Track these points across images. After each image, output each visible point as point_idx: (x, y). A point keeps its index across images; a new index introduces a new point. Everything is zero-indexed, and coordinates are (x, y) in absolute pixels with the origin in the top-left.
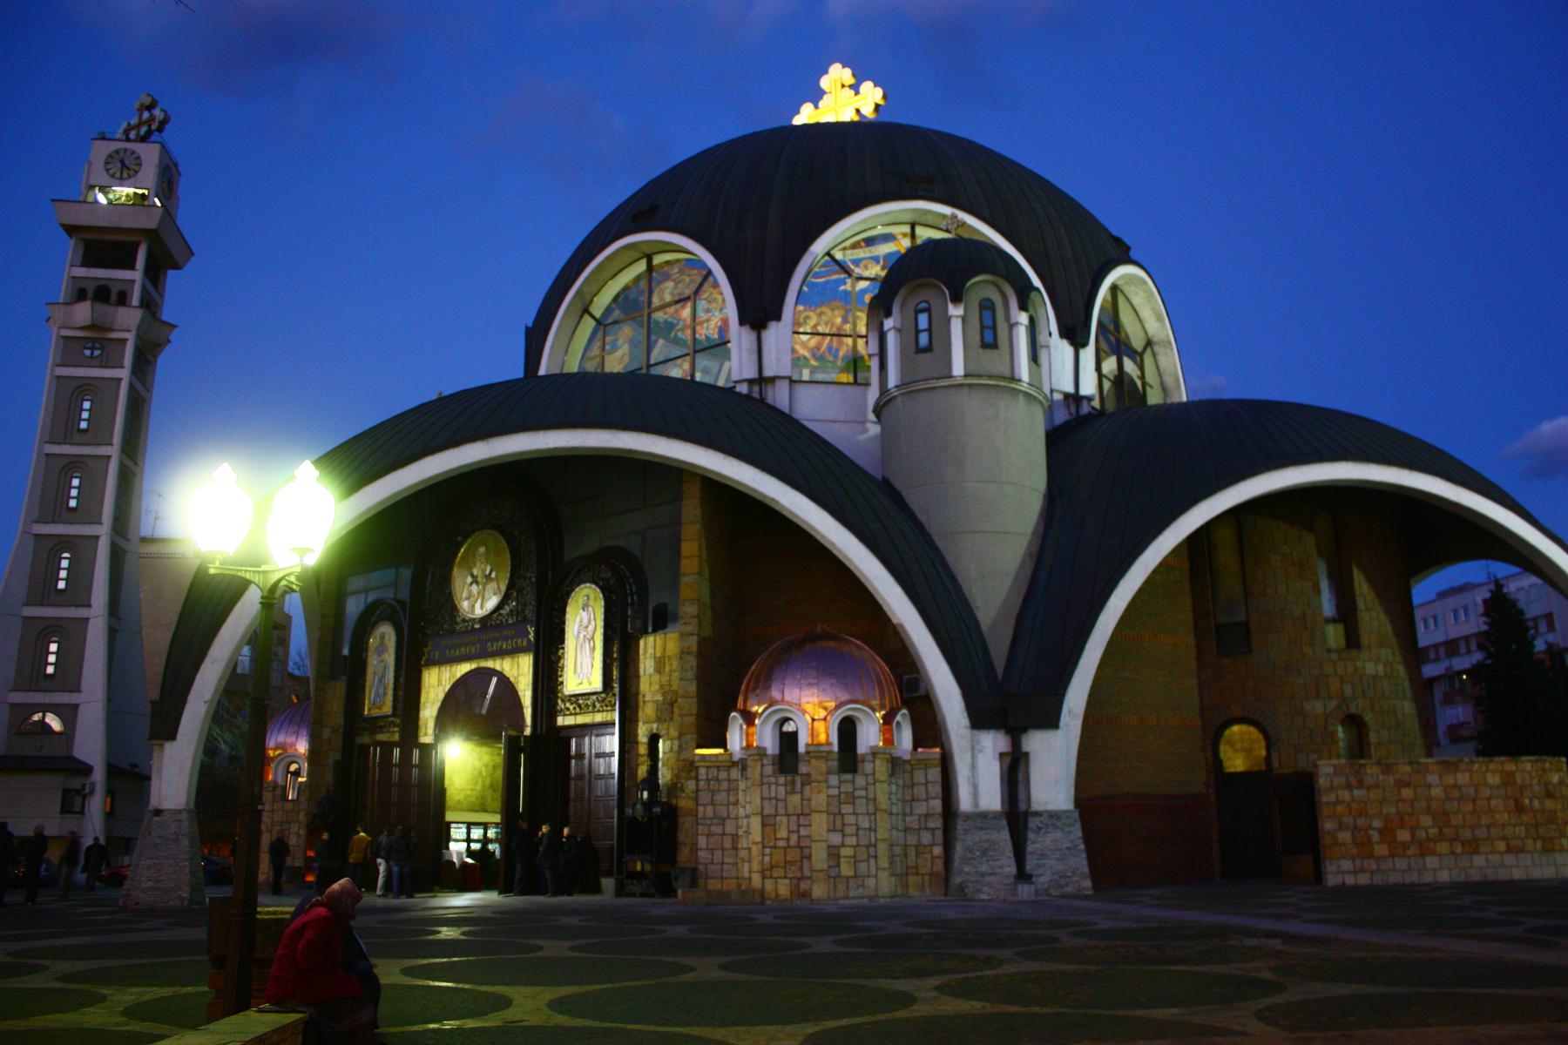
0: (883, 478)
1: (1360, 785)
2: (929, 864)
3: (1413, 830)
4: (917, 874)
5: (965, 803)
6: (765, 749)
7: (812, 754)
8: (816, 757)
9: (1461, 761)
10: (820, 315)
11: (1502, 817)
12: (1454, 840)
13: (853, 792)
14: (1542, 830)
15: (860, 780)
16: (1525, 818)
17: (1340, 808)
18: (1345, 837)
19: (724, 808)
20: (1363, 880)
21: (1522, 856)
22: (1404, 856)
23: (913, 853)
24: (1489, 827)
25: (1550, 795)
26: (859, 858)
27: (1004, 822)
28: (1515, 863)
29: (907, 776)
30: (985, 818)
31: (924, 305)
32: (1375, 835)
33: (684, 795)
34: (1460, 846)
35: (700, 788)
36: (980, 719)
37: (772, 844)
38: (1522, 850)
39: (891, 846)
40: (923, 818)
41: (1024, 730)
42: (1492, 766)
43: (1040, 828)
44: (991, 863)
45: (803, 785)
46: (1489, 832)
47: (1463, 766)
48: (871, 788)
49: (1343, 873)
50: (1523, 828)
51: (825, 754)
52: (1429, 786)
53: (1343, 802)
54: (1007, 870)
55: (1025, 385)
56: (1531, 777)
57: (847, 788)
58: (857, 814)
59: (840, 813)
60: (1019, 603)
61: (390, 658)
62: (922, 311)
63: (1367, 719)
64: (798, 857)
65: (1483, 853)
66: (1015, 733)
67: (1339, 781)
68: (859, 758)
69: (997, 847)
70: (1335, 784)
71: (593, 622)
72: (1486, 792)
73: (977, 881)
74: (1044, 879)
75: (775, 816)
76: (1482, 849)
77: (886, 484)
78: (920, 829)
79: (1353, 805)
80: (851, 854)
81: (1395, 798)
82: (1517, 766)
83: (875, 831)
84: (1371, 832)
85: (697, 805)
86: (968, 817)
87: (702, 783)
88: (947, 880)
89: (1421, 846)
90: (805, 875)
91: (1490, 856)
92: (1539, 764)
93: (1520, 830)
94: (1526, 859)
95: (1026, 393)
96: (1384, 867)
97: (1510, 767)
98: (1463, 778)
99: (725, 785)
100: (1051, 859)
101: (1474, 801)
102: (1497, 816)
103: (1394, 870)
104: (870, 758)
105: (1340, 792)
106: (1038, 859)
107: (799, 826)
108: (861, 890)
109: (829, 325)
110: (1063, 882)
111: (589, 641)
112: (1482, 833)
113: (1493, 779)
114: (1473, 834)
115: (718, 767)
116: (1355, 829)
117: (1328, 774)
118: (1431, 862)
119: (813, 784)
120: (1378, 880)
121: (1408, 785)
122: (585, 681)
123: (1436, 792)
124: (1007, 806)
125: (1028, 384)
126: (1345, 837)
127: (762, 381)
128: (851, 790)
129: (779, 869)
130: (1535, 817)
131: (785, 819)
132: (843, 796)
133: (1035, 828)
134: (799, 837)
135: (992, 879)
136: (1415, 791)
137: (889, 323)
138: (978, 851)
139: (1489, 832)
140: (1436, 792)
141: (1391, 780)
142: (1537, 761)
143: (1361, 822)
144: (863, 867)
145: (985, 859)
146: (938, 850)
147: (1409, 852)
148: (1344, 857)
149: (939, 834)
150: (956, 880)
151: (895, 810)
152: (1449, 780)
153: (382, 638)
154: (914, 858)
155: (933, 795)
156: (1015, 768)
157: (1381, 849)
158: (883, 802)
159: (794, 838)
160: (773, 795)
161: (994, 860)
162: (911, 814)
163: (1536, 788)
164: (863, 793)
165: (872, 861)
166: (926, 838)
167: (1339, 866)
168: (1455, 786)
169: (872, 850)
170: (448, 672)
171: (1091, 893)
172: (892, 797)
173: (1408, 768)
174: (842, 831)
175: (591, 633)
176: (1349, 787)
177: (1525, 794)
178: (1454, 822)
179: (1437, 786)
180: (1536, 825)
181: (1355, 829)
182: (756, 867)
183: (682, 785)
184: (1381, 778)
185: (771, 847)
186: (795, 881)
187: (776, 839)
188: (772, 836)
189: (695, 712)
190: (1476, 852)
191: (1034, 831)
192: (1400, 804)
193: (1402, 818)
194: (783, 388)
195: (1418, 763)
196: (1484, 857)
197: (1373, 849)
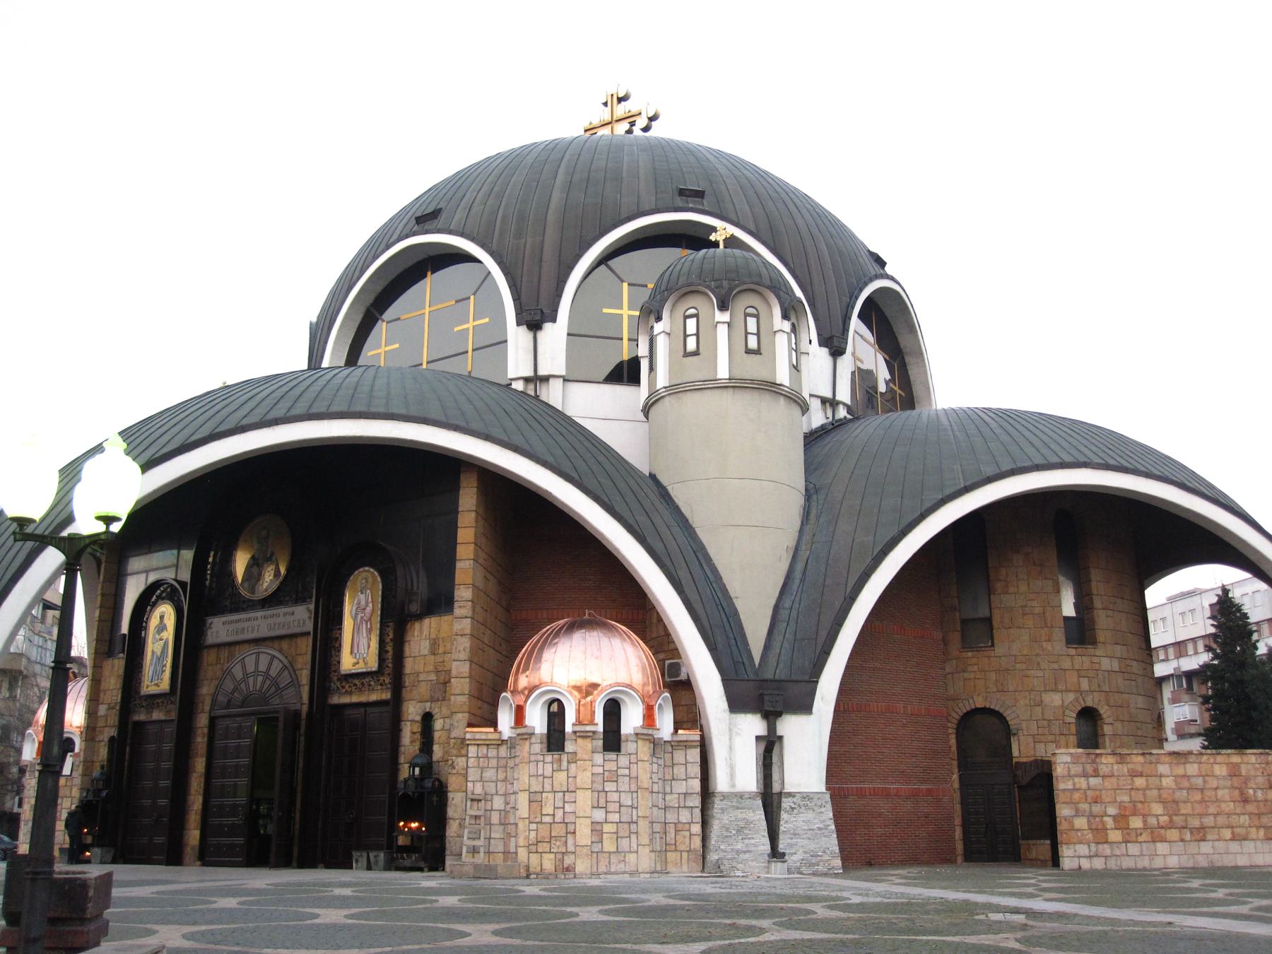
0: (650, 474)
1: (1096, 774)
2: (687, 840)
3: (1144, 816)
4: (676, 850)
6: (534, 728)
7: (578, 734)
8: (580, 737)
12: (1184, 828)
13: (617, 771)
15: (623, 760)
16: (1251, 808)
17: (1076, 796)
18: (1081, 823)
19: (494, 784)
20: (1098, 864)
22: (1137, 842)
23: (672, 831)
24: (1215, 815)
26: (621, 834)
27: (759, 802)
29: (668, 756)
30: (741, 798)
31: (692, 311)
32: (1109, 822)
33: (455, 771)
34: (1188, 833)
35: (469, 765)
36: (736, 704)
37: (538, 820)
39: (652, 823)
40: (682, 796)
41: (779, 714)
42: (1219, 759)
43: (793, 809)
44: (747, 841)
45: (568, 762)
48: (634, 767)
49: (1079, 857)
50: (1247, 817)
51: (591, 734)
54: (762, 848)
56: (1256, 769)
57: (611, 766)
58: (620, 792)
59: (604, 791)
60: (777, 594)
61: (169, 634)
62: (691, 316)
63: (1102, 712)
64: (563, 833)
65: (1209, 841)
66: (771, 716)
67: (1076, 769)
68: (623, 738)
69: (752, 825)
70: (1072, 773)
71: (371, 605)
72: (1213, 783)
73: (732, 859)
74: (794, 859)
75: (542, 793)
76: (1209, 837)
77: (653, 477)
78: (679, 807)
79: (1089, 793)
80: (615, 830)
81: (1129, 787)
83: (637, 808)
84: (1106, 819)
85: (467, 781)
86: (725, 796)
87: (471, 760)
88: (704, 858)
89: (1152, 833)
90: (569, 850)
91: (1216, 843)
92: (1263, 757)
96: (1117, 852)
97: (1236, 759)
99: (493, 763)
100: (803, 839)
104: (633, 738)
105: (1076, 780)
106: (792, 839)
107: (564, 802)
108: (622, 865)
110: (813, 861)
111: (367, 623)
113: (1221, 770)
114: (1201, 822)
115: (488, 745)
116: (1091, 816)
117: (1067, 763)
118: (1162, 848)
119: (578, 762)
120: (1112, 864)
121: (1141, 775)
122: (361, 661)
124: (762, 788)
126: (1081, 823)
127: (537, 379)
128: (615, 769)
129: (545, 844)
131: (550, 796)
132: (606, 773)
133: (788, 808)
134: (564, 813)
135: (747, 856)
136: (1147, 780)
137: (658, 327)
138: (734, 829)
140: (1168, 782)
141: (1126, 770)
143: (1097, 809)
144: (624, 843)
145: (740, 837)
146: (697, 828)
147: (1140, 839)
148: (1080, 843)
149: (697, 812)
150: (713, 857)
151: (656, 788)
153: (162, 617)
154: (674, 835)
155: (692, 775)
156: (770, 746)
157: (1115, 836)
158: (645, 780)
159: (559, 813)
160: (540, 772)
161: (750, 839)
162: (671, 793)
163: (1260, 780)
164: (626, 772)
165: (633, 837)
166: (685, 816)
167: (1075, 851)
168: (1184, 776)
169: (633, 827)
170: (227, 651)
171: (841, 871)
172: (654, 776)
173: (1140, 759)
174: (606, 808)
175: (368, 615)
176: (1085, 775)
178: (1183, 811)
179: (1168, 776)
180: (1259, 815)
181: (1091, 816)
182: (521, 842)
183: (453, 762)
185: (537, 823)
186: (559, 856)
187: (542, 815)
188: (539, 812)
189: (467, 692)
191: (787, 812)
192: (1133, 793)
193: (1134, 806)
194: (556, 385)
197: (1107, 835)
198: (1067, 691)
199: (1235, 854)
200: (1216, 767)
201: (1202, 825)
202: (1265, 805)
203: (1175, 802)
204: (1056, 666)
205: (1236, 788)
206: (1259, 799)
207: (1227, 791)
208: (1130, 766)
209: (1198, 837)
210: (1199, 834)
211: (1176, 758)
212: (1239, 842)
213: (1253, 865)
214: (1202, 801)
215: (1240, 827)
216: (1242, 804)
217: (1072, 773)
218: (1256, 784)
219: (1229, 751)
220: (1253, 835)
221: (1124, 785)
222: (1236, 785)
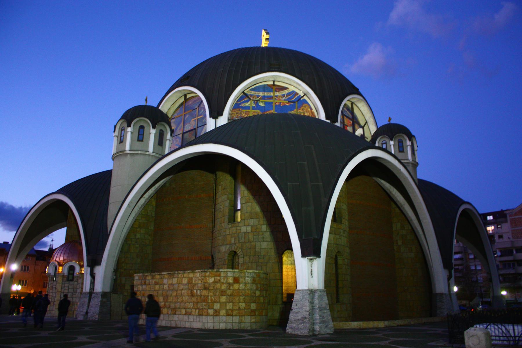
5: (84, 291)
9: (175, 273)
10: (303, 110)
11: (186, 298)
12: (169, 308)
14: (199, 305)
15: (55, 283)
16: (194, 299)
21: (190, 317)
25: (205, 288)
27: (88, 295)
28: (187, 320)
34: (170, 310)
38: (190, 314)
42: (185, 275)
43: (93, 298)
46: (180, 306)
47: (176, 275)
50: (192, 304)
52: (164, 284)
53: (139, 291)
55: (128, 151)
65: (177, 314)
67: (139, 282)
72: (181, 287)
76: (177, 313)
79: (142, 292)
81: (153, 289)
82: (194, 274)
91: (179, 316)
92: (203, 273)
93: (191, 305)
94: (191, 318)
95: (130, 154)
97: (191, 275)
98: (175, 281)
101: (177, 291)
102: (184, 298)
103: (166, 320)
109: (308, 112)
112: (178, 305)
113: (185, 281)
114: (175, 305)
117: (137, 280)
123: (166, 287)
125: (129, 150)
130: (197, 299)
136: (159, 286)
139: (180, 306)
141: (153, 282)
142: (202, 272)
152: (170, 282)
173: (158, 277)
176: (142, 285)
177: (195, 288)
178: (169, 300)
179: (167, 284)
180: (197, 303)
184: (151, 281)
190: (175, 314)
195: (161, 274)
196: (177, 315)
198: (227, 244)
199: (186, 321)
200: (184, 279)
201: (175, 307)
202: (200, 298)
203: (167, 296)
204: (224, 234)
205: (190, 289)
206: (198, 295)
207: (186, 291)
208: (155, 280)
209: (173, 312)
210: (173, 311)
211: (170, 276)
212: (188, 316)
213: (191, 327)
214: (176, 296)
215: (189, 308)
216: (191, 297)
217: (138, 284)
218: (197, 287)
219: (189, 271)
220: (193, 313)
221: (152, 289)
222: (189, 288)
